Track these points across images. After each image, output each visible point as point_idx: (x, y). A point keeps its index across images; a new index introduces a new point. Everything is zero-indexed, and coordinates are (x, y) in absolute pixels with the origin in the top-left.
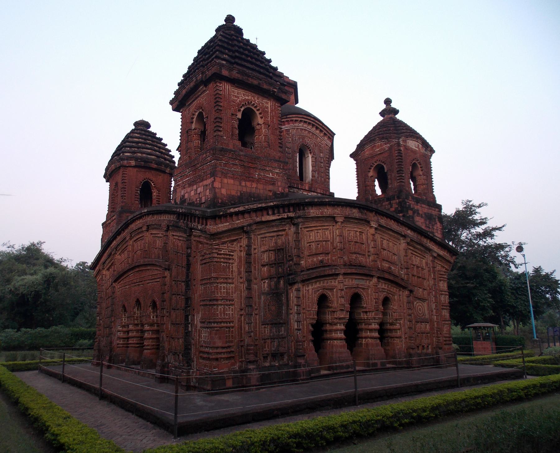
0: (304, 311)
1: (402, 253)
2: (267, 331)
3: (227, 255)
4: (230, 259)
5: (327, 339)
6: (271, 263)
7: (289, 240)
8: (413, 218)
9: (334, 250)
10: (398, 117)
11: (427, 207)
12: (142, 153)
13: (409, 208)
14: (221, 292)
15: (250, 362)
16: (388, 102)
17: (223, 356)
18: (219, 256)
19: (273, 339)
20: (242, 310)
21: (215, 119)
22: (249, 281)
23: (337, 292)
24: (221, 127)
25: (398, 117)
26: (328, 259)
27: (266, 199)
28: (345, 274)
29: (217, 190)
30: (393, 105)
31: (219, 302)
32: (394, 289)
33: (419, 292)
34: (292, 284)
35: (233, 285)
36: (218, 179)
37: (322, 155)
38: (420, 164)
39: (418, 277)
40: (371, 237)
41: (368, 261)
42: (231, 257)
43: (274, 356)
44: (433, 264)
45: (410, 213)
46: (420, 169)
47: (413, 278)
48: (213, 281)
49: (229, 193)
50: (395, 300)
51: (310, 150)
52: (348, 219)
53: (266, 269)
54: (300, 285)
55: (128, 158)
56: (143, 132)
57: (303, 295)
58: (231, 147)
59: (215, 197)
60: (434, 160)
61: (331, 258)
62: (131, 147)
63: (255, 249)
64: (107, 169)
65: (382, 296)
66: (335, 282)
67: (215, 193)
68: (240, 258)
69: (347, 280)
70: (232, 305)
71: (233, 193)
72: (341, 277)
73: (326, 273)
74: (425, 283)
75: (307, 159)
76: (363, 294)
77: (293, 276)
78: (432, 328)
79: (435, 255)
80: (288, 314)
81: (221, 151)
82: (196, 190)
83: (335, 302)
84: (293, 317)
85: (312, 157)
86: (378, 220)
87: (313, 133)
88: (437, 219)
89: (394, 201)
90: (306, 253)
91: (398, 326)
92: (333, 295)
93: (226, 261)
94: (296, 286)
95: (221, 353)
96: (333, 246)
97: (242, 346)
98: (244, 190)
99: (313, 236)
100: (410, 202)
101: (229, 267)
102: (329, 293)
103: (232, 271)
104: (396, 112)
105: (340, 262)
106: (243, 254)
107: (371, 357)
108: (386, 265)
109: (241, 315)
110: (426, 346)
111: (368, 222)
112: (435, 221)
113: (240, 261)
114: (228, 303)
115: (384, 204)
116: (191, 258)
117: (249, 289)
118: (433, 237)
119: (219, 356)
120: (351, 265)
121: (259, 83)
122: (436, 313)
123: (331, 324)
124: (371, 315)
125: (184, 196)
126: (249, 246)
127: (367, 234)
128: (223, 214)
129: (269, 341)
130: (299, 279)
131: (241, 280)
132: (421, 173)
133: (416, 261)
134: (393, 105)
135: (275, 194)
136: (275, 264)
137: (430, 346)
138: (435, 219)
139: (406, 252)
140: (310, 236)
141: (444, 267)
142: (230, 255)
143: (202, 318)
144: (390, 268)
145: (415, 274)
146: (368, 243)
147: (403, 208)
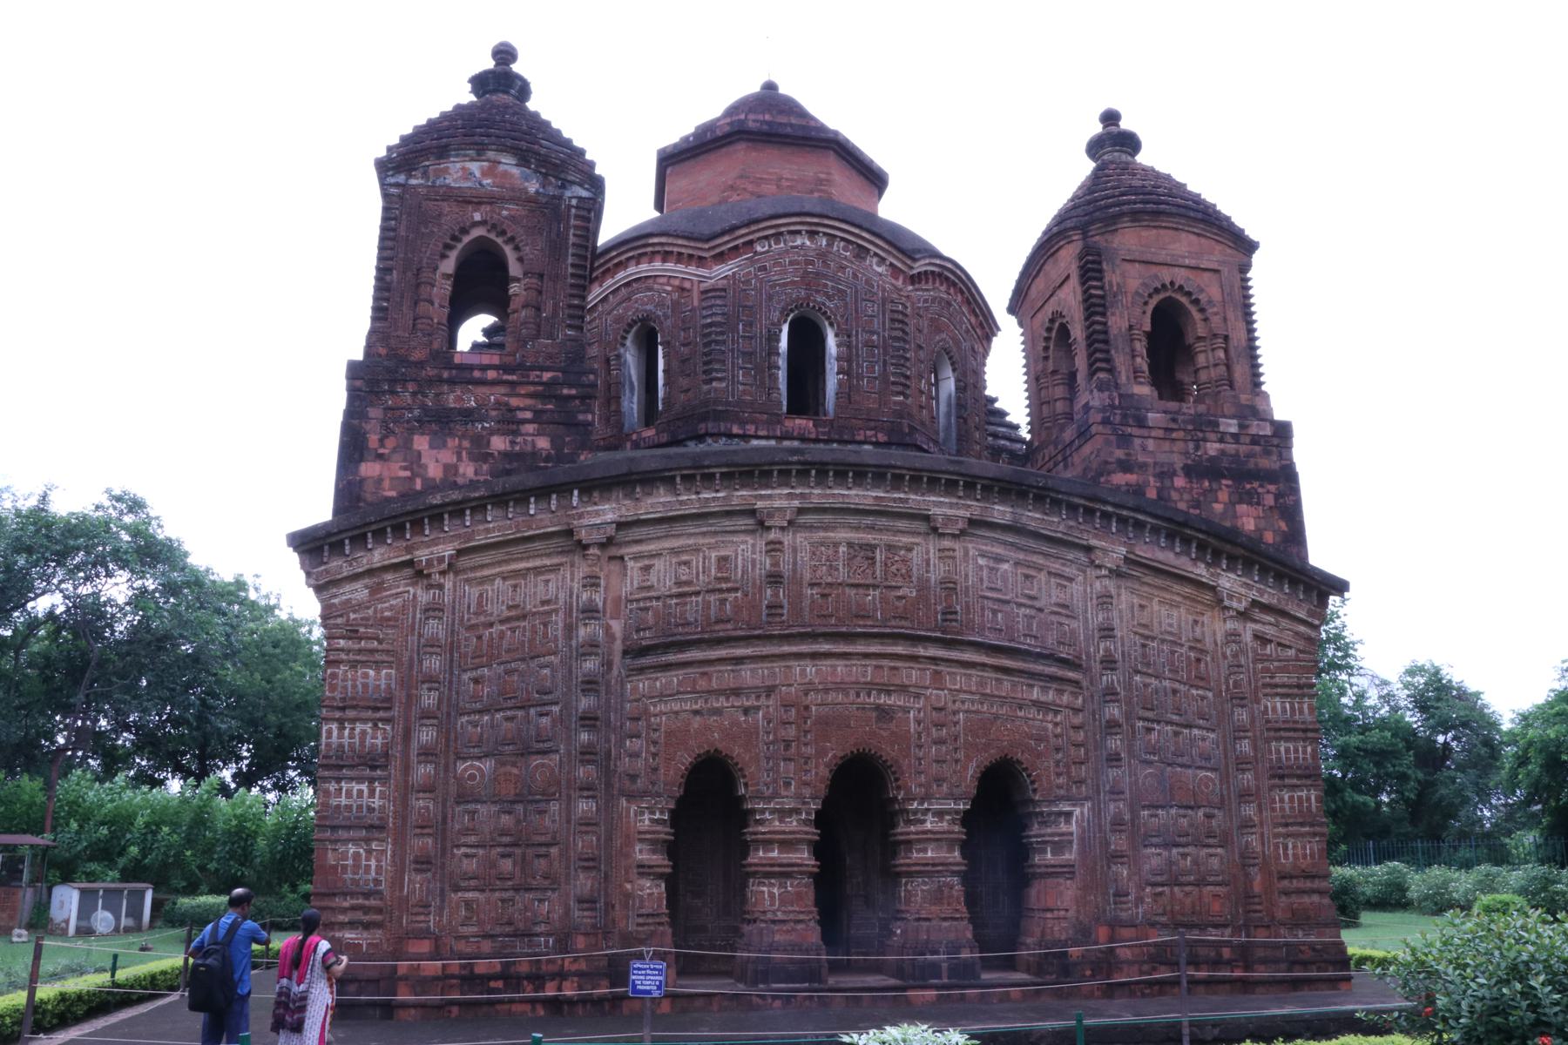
10: (1142, 158)
16: (1110, 118)
25: (1142, 158)
30: (1125, 125)
46: (1197, 316)
51: (828, 318)
60: (1262, 276)
85: (837, 335)
104: (1130, 143)
134: (1125, 125)
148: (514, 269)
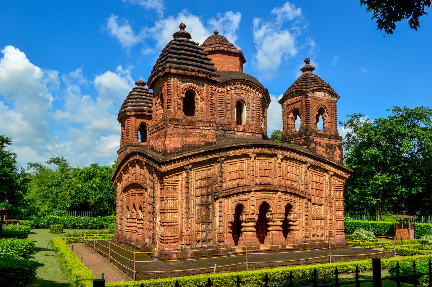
0: (225, 215)
1: (304, 174)
2: (199, 227)
3: (173, 183)
4: (175, 186)
5: (243, 232)
6: (202, 186)
7: (215, 171)
8: (315, 148)
9: (248, 176)
11: (328, 139)
12: (139, 106)
13: (313, 141)
14: (170, 205)
15: (187, 245)
17: (170, 241)
18: (168, 184)
19: (203, 231)
20: (182, 215)
21: (167, 100)
22: (188, 198)
23: (249, 202)
24: (170, 106)
26: (243, 182)
27: (200, 147)
28: (255, 191)
29: (167, 146)
31: (168, 211)
32: (295, 199)
33: (314, 199)
34: (216, 199)
35: (177, 201)
36: (168, 139)
37: (254, 105)
38: (326, 108)
39: (316, 189)
40: (278, 165)
41: (275, 181)
42: (176, 184)
43: (204, 241)
44: (330, 180)
45: (313, 145)
47: (313, 190)
48: (165, 199)
49: (175, 146)
50: (296, 206)
52: (259, 155)
53: (199, 190)
54: (223, 200)
55: (130, 111)
56: (140, 90)
57: (224, 205)
58: (177, 117)
59: (166, 150)
61: (246, 181)
62: (132, 102)
63: (192, 179)
64: (119, 116)
65: (284, 204)
66: (248, 196)
67: (166, 147)
68: (182, 184)
69: (257, 194)
70: (177, 212)
71: (178, 146)
72: (252, 193)
73: (241, 191)
74: (323, 194)
76: (270, 202)
77: (217, 194)
78: (327, 224)
79: (332, 173)
80: (214, 217)
81: (170, 121)
82: (158, 143)
83: (248, 209)
84: (217, 219)
86: (283, 153)
87: (247, 91)
88: (337, 148)
89: (302, 138)
90: (227, 179)
91: (297, 223)
92: (247, 204)
93: (173, 187)
94: (219, 200)
95: (169, 240)
96: (248, 173)
97: (183, 236)
98: (185, 143)
99: (233, 168)
100: (314, 137)
101: (175, 191)
102: (244, 203)
103: (177, 193)
104: (312, 69)
105: (252, 183)
106: (184, 182)
107: (274, 242)
108: (289, 183)
109: (182, 218)
110: (320, 236)
111: (275, 156)
112: (335, 149)
113: (182, 187)
114: (174, 211)
115: (297, 138)
116: (155, 184)
117: (187, 203)
119: (168, 241)
120: (261, 185)
121: (196, 74)
122: (330, 213)
123: (245, 222)
124: (275, 216)
125: (153, 145)
126: (188, 178)
127: (275, 163)
128: (169, 161)
129: (200, 233)
130: (221, 195)
131: (183, 198)
132: (327, 115)
133: (316, 178)
135: (206, 144)
136: (205, 187)
137: (324, 236)
138: (335, 147)
139: (306, 173)
140: (231, 168)
141: (340, 181)
142: (175, 183)
143: (161, 220)
144: (292, 185)
145: (314, 187)
146: (275, 169)
147: (308, 142)
148: (197, 96)
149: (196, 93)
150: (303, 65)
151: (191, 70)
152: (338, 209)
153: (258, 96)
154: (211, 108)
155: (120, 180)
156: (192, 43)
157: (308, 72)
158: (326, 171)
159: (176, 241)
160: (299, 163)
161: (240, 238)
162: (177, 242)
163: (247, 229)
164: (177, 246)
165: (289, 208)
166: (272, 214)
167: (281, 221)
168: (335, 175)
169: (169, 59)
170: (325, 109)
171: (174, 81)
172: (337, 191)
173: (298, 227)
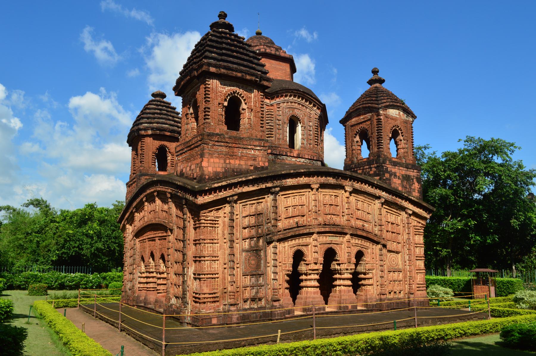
0: (281, 264)
1: (377, 212)
2: (248, 280)
3: (213, 221)
4: (215, 224)
5: (303, 287)
6: (251, 225)
7: (267, 206)
8: (390, 180)
9: (310, 213)
11: (405, 169)
12: (158, 123)
13: (387, 171)
14: (208, 250)
15: (231, 305)
16: (375, 72)
17: (209, 300)
18: (206, 222)
19: (252, 287)
20: (225, 264)
21: (205, 109)
22: (232, 241)
23: (311, 248)
24: (209, 115)
25: (384, 85)
26: (304, 221)
27: (247, 172)
28: (319, 233)
29: (204, 169)
31: (206, 258)
32: (368, 244)
33: (391, 246)
34: (269, 243)
35: (218, 245)
36: (205, 160)
37: (311, 123)
38: (401, 130)
39: (392, 232)
40: (346, 199)
41: (342, 221)
42: (216, 222)
43: (253, 300)
44: (408, 220)
45: (387, 175)
47: (388, 233)
48: (201, 241)
49: (215, 170)
50: (368, 253)
52: (323, 186)
53: (246, 230)
54: (277, 244)
55: (146, 129)
56: (159, 103)
57: (280, 251)
58: (217, 131)
59: (202, 175)
61: (306, 219)
62: (148, 118)
63: (237, 215)
64: (129, 136)
65: (354, 250)
66: (310, 240)
67: (203, 171)
68: (224, 222)
69: (321, 237)
70: (218, 260)
71: (219, 170)
72: (315, 236)
73: (301, 232)
74: (400, 238)
75: (297, 128)
76: (337, 248)
77: (270, 236)
78: (405, 277)
79: (411, 212)
80: (266, 267)
81: (208, 136)
82: (190, 167)
83: (310, 256)
84: (270, 270)
85: (302, 126)
86: (353, 184)
87: (302, 105)
88: (415, 180)
89: (373, 166)
90: (283, 216)
91: (370, 276)
92: (308, 250)
93: (212, 225)
94: (273, 244)
95: (207, 298)
96: (308, 209)
97: (225, 293)
98: (228, 166)
99: (291, 201)
100: (388, 166)
101: (215, 231)
102: (304, 249)
103: (218, 233)
105: (314, 222)
106: (227, 220)
107: (342, 301)
108: (359, 223)
109: (225, 268)
110: (398, 292)
111: (342, 187)
112: (413, 181)
113: (224, 225)
114: (214, 259)
115: (365, 167)
116: (186, 222)
117: (231, 247)
118: (407, 197)
119: (206, 300)
120: (325, 225)
121: (243, 76)
122: (409, 263)
123: (306, 274)
124: (343, 267)
125: (182, 170)
126: (232, 213)
127: (342, 197)
128: (208, 189)
129: (249, 288)
130: (276, 238)
131: (225, 241)
132: (402, 138)
133: (392, 218)
134: (381, 75)
135: (256, 168)
136: (255, 226)
137: (402, 292)
138: (413, 179)
139: (380, 211)
140: (287, 202)
141: (420, 223)
142: (215, 221)
143: (195, 270)
144: (363, 226)
145: (390, 230)
146: (342, 205)
147: (381, 171)
148: (243, 106)
149: (242, 101)
150: (371, 76)
151: (237, 70)
152: (418, 258)
153: (316, 112)
154: (262, 122)
155: (131, 221)
156: (236, 36)
157: (377, 85)
158: (403, 209)
159: (216, 299)
160: (372, 198)
161: (298, 296)
162: (218, 301)
163: (308, 283)
164: (218, 306)
165: (359, 255)
166: (339, 264)
167: (350, 273)
168: (415, 214)
169: (207, 54)
170: (400, 132)
171: (214, 83)
172: (416, 234)
173: (370, 282)
